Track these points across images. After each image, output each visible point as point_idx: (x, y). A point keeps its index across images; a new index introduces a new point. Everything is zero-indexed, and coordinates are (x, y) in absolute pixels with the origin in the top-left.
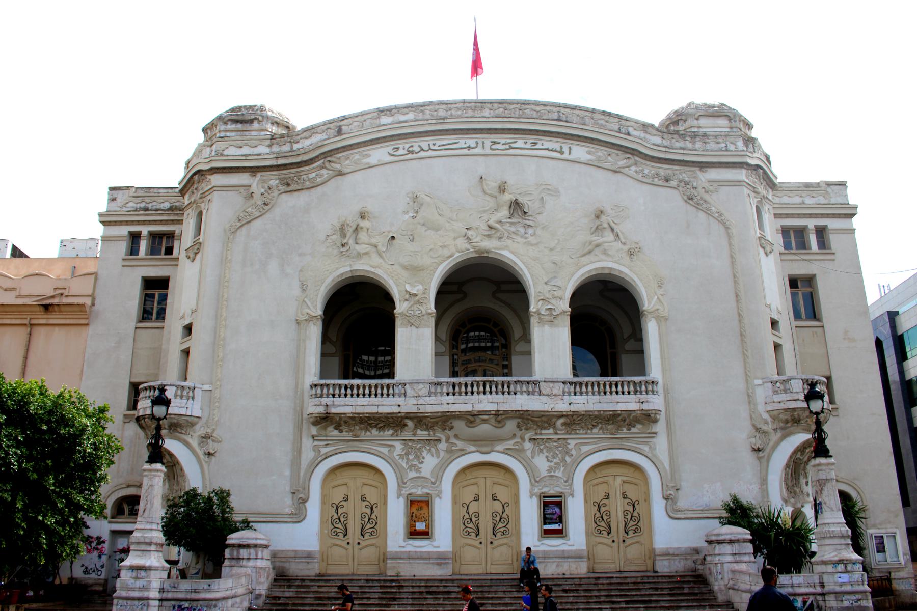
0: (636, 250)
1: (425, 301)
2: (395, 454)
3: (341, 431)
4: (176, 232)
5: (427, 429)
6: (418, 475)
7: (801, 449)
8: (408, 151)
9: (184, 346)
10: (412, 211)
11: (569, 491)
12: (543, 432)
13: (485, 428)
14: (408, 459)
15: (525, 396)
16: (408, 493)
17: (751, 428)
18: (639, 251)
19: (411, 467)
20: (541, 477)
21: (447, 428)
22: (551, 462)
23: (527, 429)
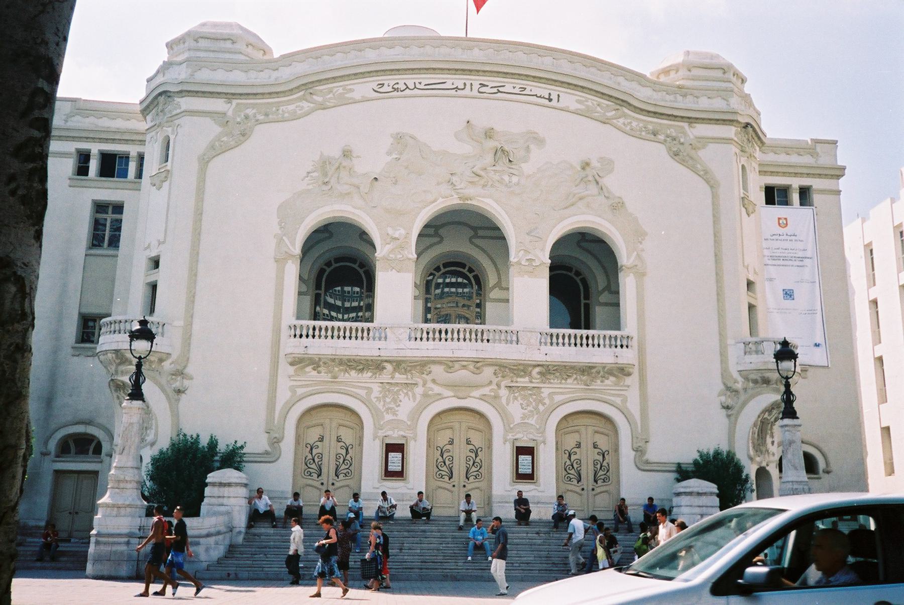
0: (619, 205)
2: (373, 396)
3: (319, 372)
4: (131, 154)
6: (395, 418)
7: (769, 410)
8: (393, 88)
9: (151, 279)
10: (396, 152)
11: (541, 439)
12: (519, 379)
13: (464, 373)
14: (385, 401)
15: (503, 345)
16: (384, 435)
17: (722, 387)
18: (621, 206)
19: (388, 410)
20: (516, 423)
21: (426, 373)
22: (526, 409)
23: (503, 377)
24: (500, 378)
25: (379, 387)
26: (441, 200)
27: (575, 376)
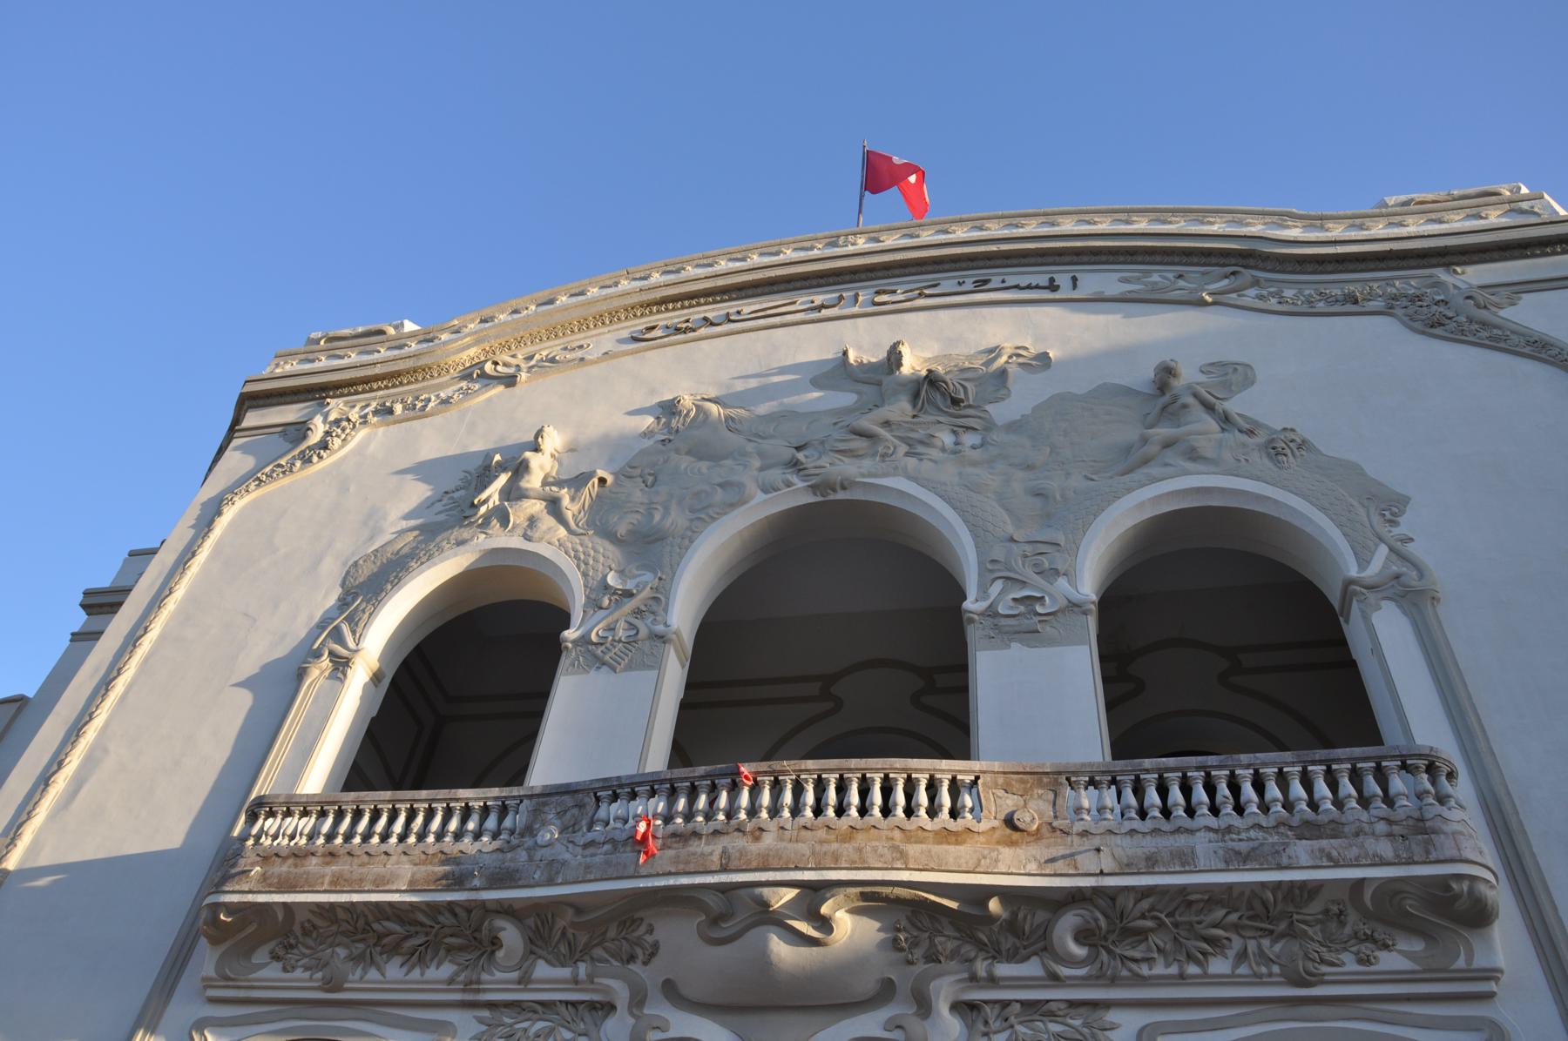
1: (655, 608)
5: (572, 954)
12: (1004, 970)
21: (639, 951)
23: (932, 957)
24: (921, 967)
25: (481, 1021)
26: (760, 496)
27: (1237, 943)
